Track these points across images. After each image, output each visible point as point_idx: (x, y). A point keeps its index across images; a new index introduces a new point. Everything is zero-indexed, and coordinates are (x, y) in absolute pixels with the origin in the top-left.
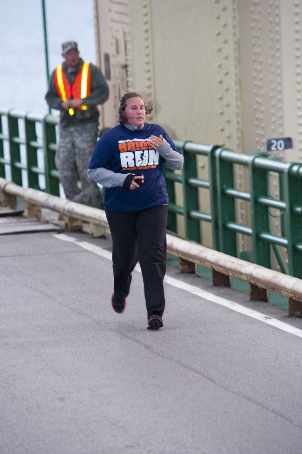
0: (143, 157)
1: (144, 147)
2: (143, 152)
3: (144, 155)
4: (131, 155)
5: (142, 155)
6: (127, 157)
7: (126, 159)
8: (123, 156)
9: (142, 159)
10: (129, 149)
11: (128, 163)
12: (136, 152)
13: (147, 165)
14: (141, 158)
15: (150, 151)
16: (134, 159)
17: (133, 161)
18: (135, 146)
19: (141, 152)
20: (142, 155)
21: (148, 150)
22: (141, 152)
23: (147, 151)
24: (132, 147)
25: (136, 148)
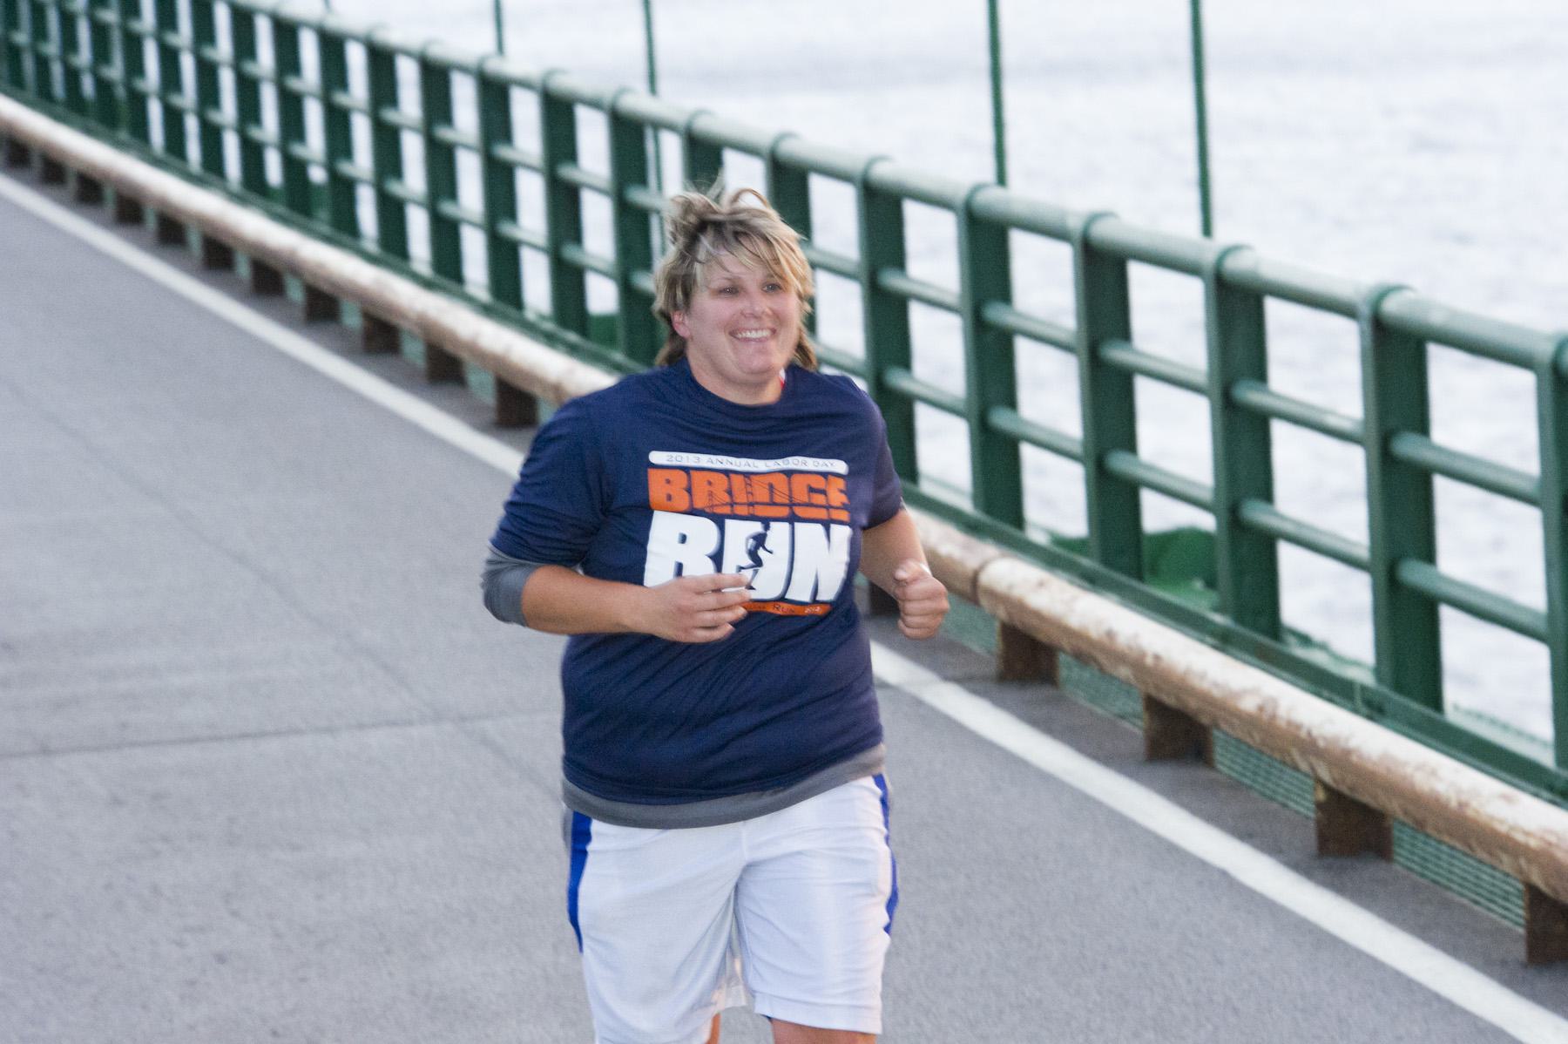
0: (761, 553)
2: (767, 527)
4: (703, 531)
5: (760, 540)
7: (676, 546)
9: (758, 563)
10: (699, 505)
12: (729, 523)
14: (753, 554)
15: (798, 525)
18: (730, 492)
19: (757, 527)
20: (760, 540)
21: (792, 519)
23: (786, 525)
24: (711, 494)
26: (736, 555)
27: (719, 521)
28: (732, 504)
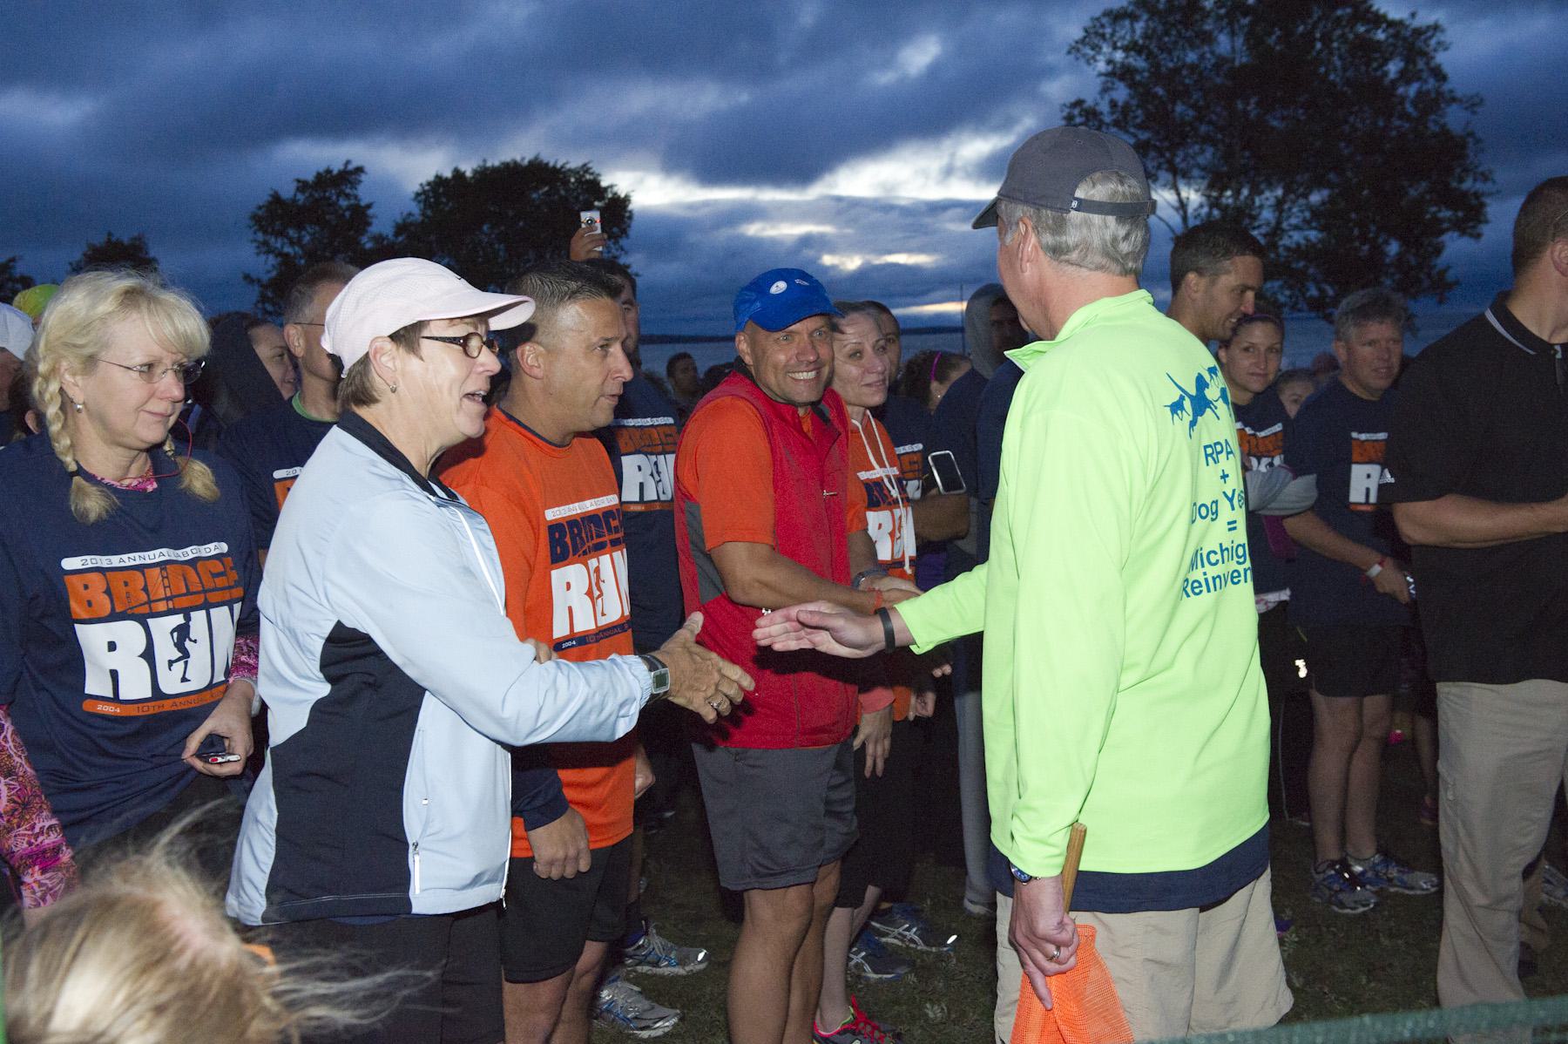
0: (188, 644)
1: (189, 593)
2: (188, 618)
3: (192, 636)
4: (129, 633)
5: (182, 632)
6: (112, 646)
9: (185, 655)
14: (180, 645)
16: (149, 655)
17: (144, 664)
19: (178, 619)
20: (182, 632)
22: (178, 619)
25: (149, 602)
26: (165, 649)
27: (142, 620)
28: (149, 602)
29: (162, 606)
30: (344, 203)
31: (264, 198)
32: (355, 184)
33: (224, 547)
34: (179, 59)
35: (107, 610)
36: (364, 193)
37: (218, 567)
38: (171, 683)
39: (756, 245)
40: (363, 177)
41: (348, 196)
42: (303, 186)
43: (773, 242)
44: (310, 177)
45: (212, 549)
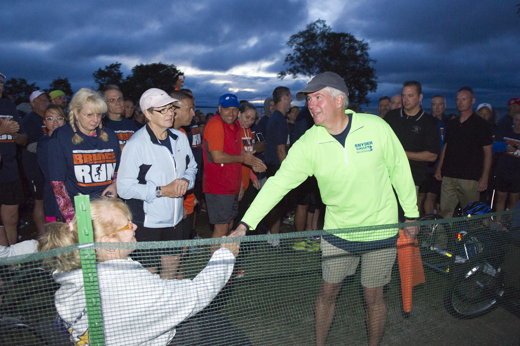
0: (100, 171)
2: (101, 166)
4: (87, 168)
5: (99, 168)
6: (83, 171)
8: (78, 169)
9: (99, 174)
11: (83, 177)
13: (106, 181)
14: (98, 171)
15: (107, 164)
16: (90, 173)
19: (99, 166)
20: (99, 168)
21: (106, 163)
22: (99, 166)
25: (93, 161)
26: (94, 172)
27: (90, 166)
29: (96, 162)
30: (116, 72)
31: (97, 70)
32: (119, 68)
33: (112, 150)
34: (73, 35)
35: (82, 163)
36: (121, 70)
37: (110, 154)
38: (96, 179)
39: (213, 85)
40: (121, 66)
41: (117, 71)
42: (107, 68)
43: (217, 84)
44: (109, 65)
45: (109, 150)
